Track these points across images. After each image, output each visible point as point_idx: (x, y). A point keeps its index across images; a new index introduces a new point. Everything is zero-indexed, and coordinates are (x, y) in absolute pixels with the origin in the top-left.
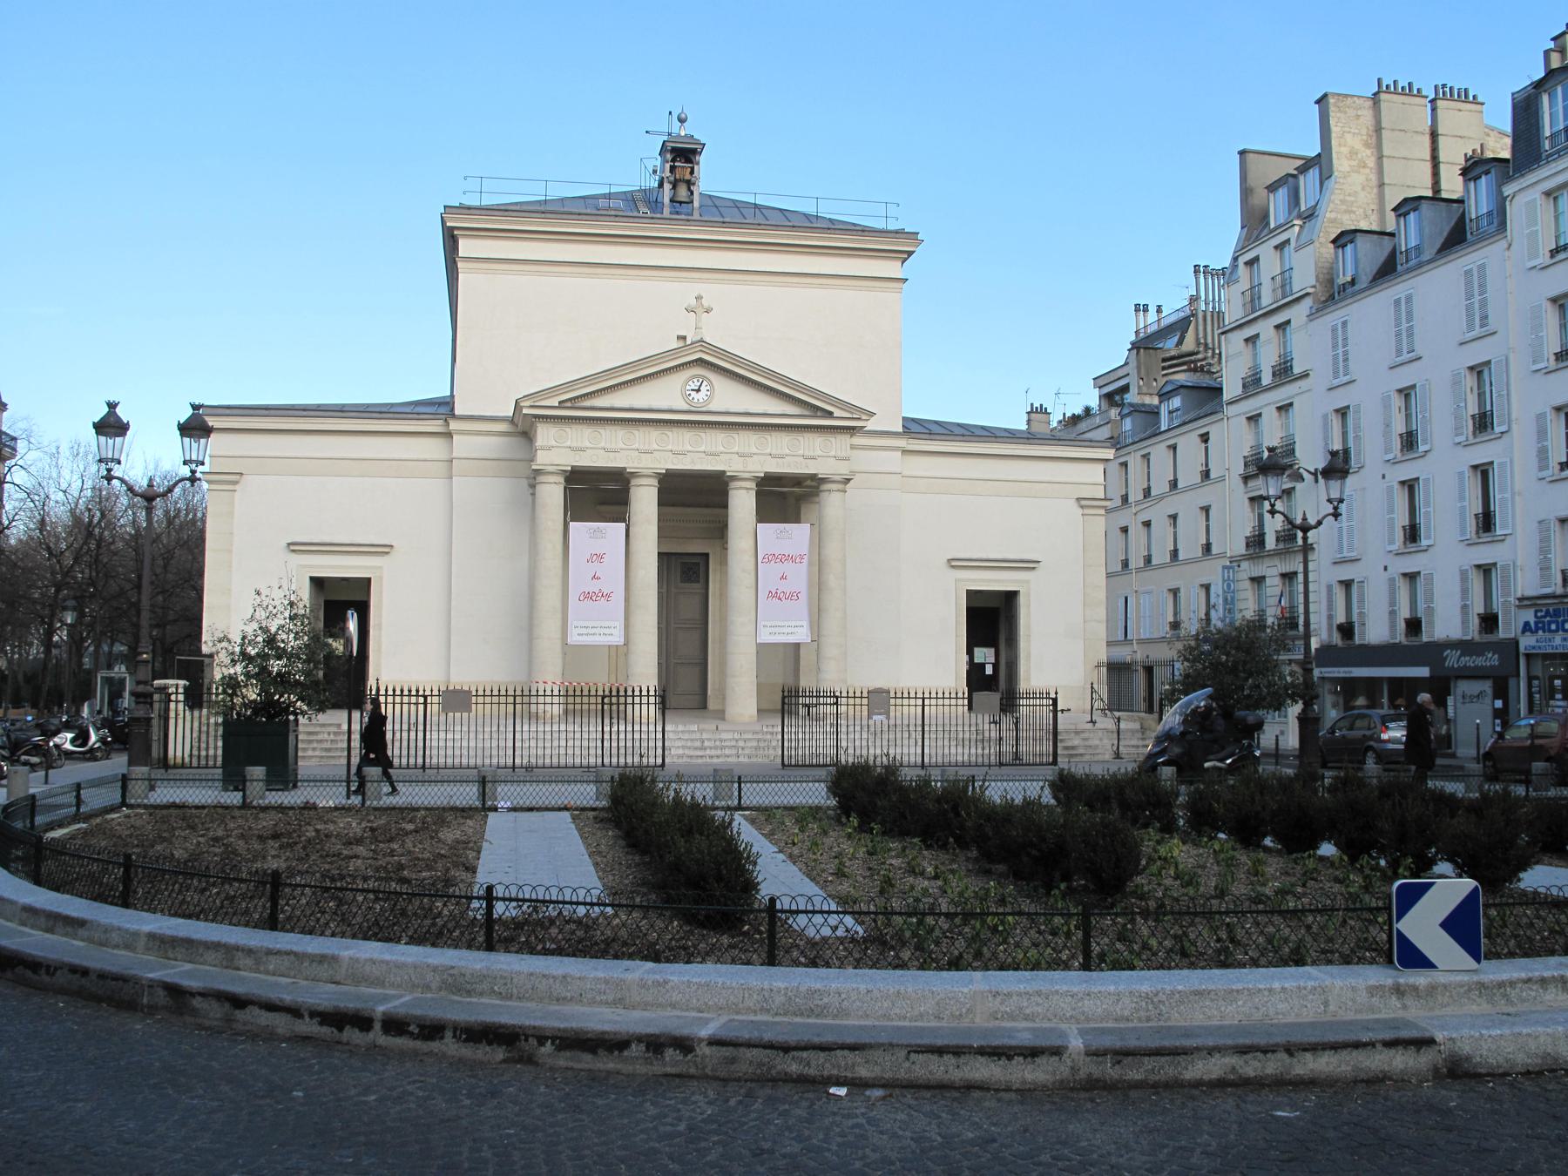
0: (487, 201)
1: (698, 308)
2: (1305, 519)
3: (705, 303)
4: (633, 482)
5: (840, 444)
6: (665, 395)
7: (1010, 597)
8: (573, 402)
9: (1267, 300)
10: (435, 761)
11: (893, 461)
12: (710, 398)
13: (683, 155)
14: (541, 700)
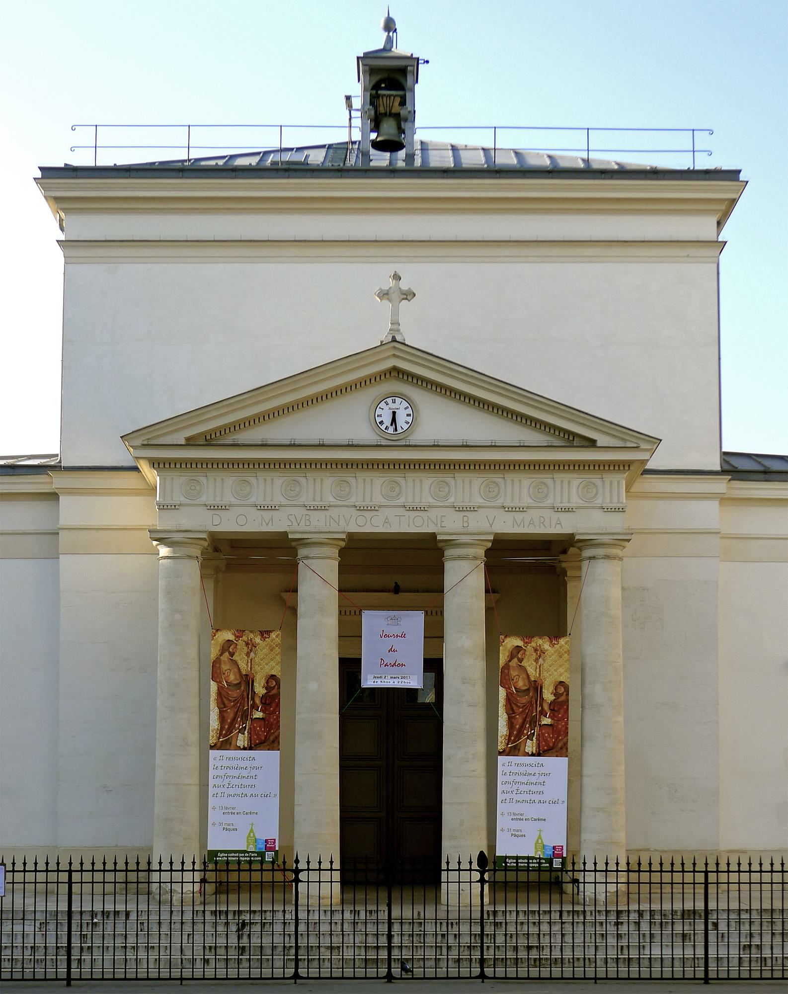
3: (404, 285)
4: (302, 552)
6: (348, 423)
8: (208, 440)
10: (86, 969)
13: (389, 82)
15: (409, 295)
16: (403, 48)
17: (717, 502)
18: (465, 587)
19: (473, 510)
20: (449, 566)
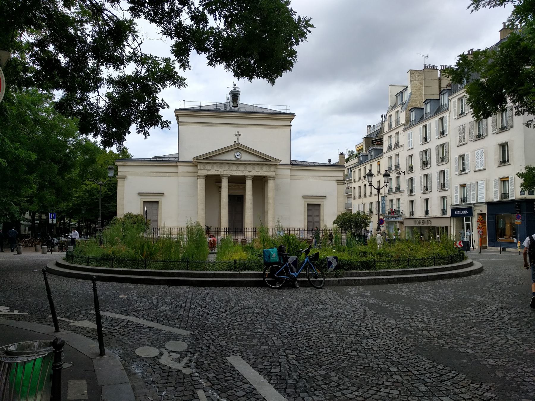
0: (186, 107)
1: (238, 135)
5: (273, 169)
6: (230, 157)
8: (207, 159)
9: (394, 126)
11: (288, 172)
12: (240, 158)
15: (240, 135)
17: (289, 170)
18: (249, 184)
20: (247, 180)
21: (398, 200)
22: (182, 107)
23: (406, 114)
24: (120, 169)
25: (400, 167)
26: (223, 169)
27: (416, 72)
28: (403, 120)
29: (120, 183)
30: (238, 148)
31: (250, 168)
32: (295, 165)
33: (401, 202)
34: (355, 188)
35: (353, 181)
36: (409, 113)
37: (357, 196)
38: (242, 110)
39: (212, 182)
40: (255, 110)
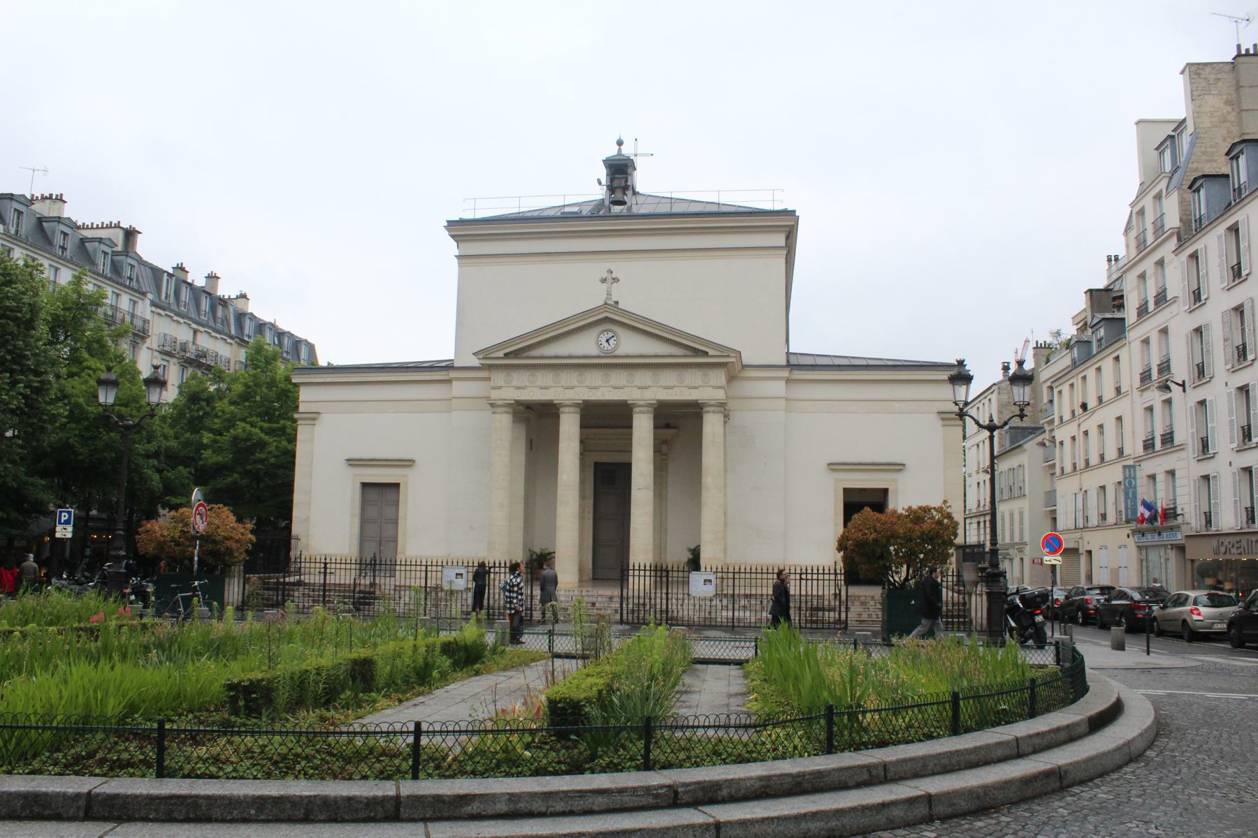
0: (479, 215)
2: (991, 420)
5: (719, 377)
6: (585, 345)
7: (886, 491)
8: (515, 354)
9: (1150, 238)
11: (779, 388)
13: (620, 171)
14: (742, 576)
15: (616, 280)
16: (627, 151)
18: (643, 427)
19: (646, 388)
21: (1172, 473)
22: (469, 215)
23: (1182, 202)
24: (305, 395)
25: (1173, 369)
26: (563, 383)
27: (1208, 69)
28: (1173, 220)
29: (303, 433)
30: (608, 318)
31: (643, 377)
32: (800, 368)
33: (1178, 483)
34: (1061, 443)
35: (1057, 422)
36: (1189, 195)
37: (1068, 469)
38: (643, 211)
39: (537, 420)
40: (677, 209)
